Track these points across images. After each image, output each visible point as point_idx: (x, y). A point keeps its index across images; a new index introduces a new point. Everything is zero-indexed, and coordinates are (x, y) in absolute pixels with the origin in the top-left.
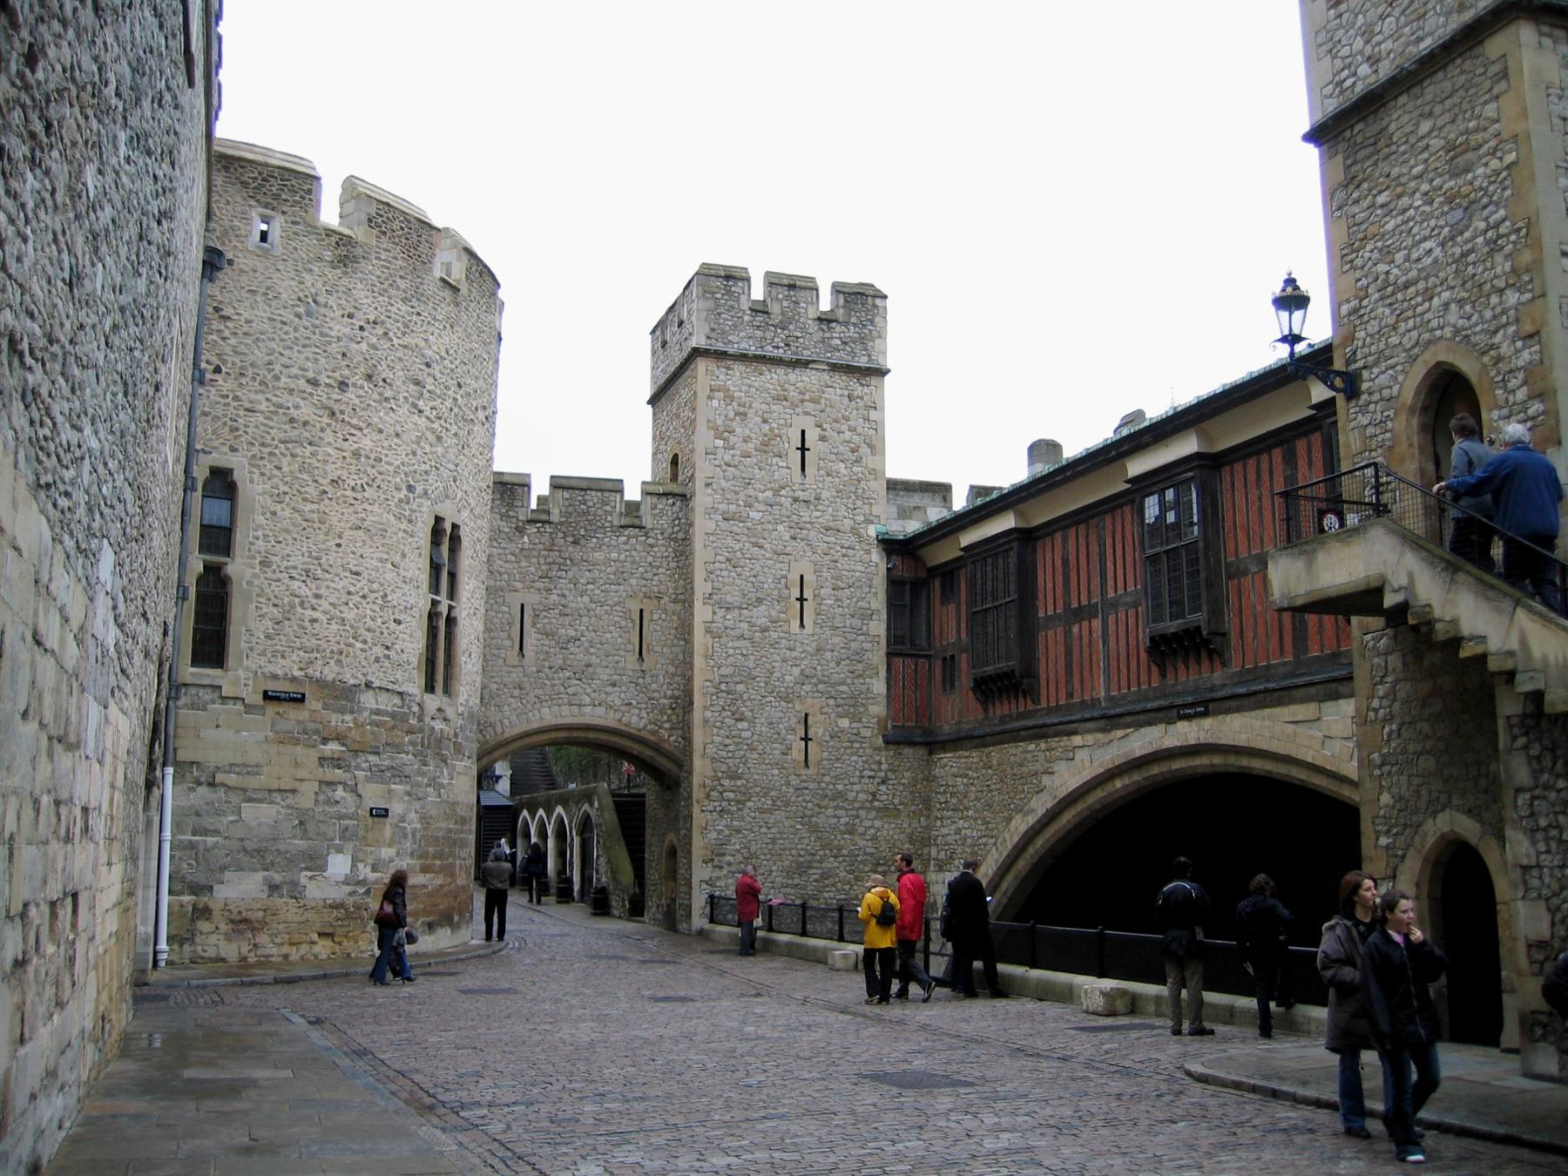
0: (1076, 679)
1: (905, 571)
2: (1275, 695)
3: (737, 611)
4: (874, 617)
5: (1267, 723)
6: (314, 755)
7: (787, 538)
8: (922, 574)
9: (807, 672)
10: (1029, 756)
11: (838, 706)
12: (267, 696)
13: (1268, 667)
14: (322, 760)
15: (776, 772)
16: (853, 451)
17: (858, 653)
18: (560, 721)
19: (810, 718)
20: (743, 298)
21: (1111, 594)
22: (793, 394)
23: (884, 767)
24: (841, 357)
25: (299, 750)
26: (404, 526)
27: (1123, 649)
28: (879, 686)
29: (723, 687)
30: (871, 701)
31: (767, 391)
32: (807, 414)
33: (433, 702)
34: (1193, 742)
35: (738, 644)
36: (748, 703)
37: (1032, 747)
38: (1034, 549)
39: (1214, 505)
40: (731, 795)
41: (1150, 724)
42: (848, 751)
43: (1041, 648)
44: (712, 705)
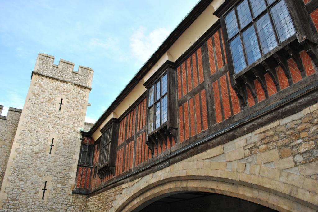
0: (126, 164)
1: (87, 142)
2: (199, 148)
3: (28, 146)
4: (75, 154)
5: (195, 162)
7: (51, 127)
8: (93, 143)
9: (49, 168)
10: (110, 194)
11: (58, 180)
13: (196, 137)
15: (31, 200)
16: (77, 107)
17: (68, 164)
19: (47, 183)
20: (51, 63)
21: (138, 130)
22: (61, 89)
23: (71, 201)
24: (76, 82)
27: (140, 149)
28: (74, 175)
29: (17, 169)
30: (70, 179)
31: (53, 87)
32: (64, 95)
34: (162, 178)
35: (26, 156)
36: (25, 176)
37: (111, 191)
38: (119, 126)
39: (174, 80)
40: (12, 207)
41: (147, 174)
42: (59, 195)
43: (117, 157)
44: (12, 175)
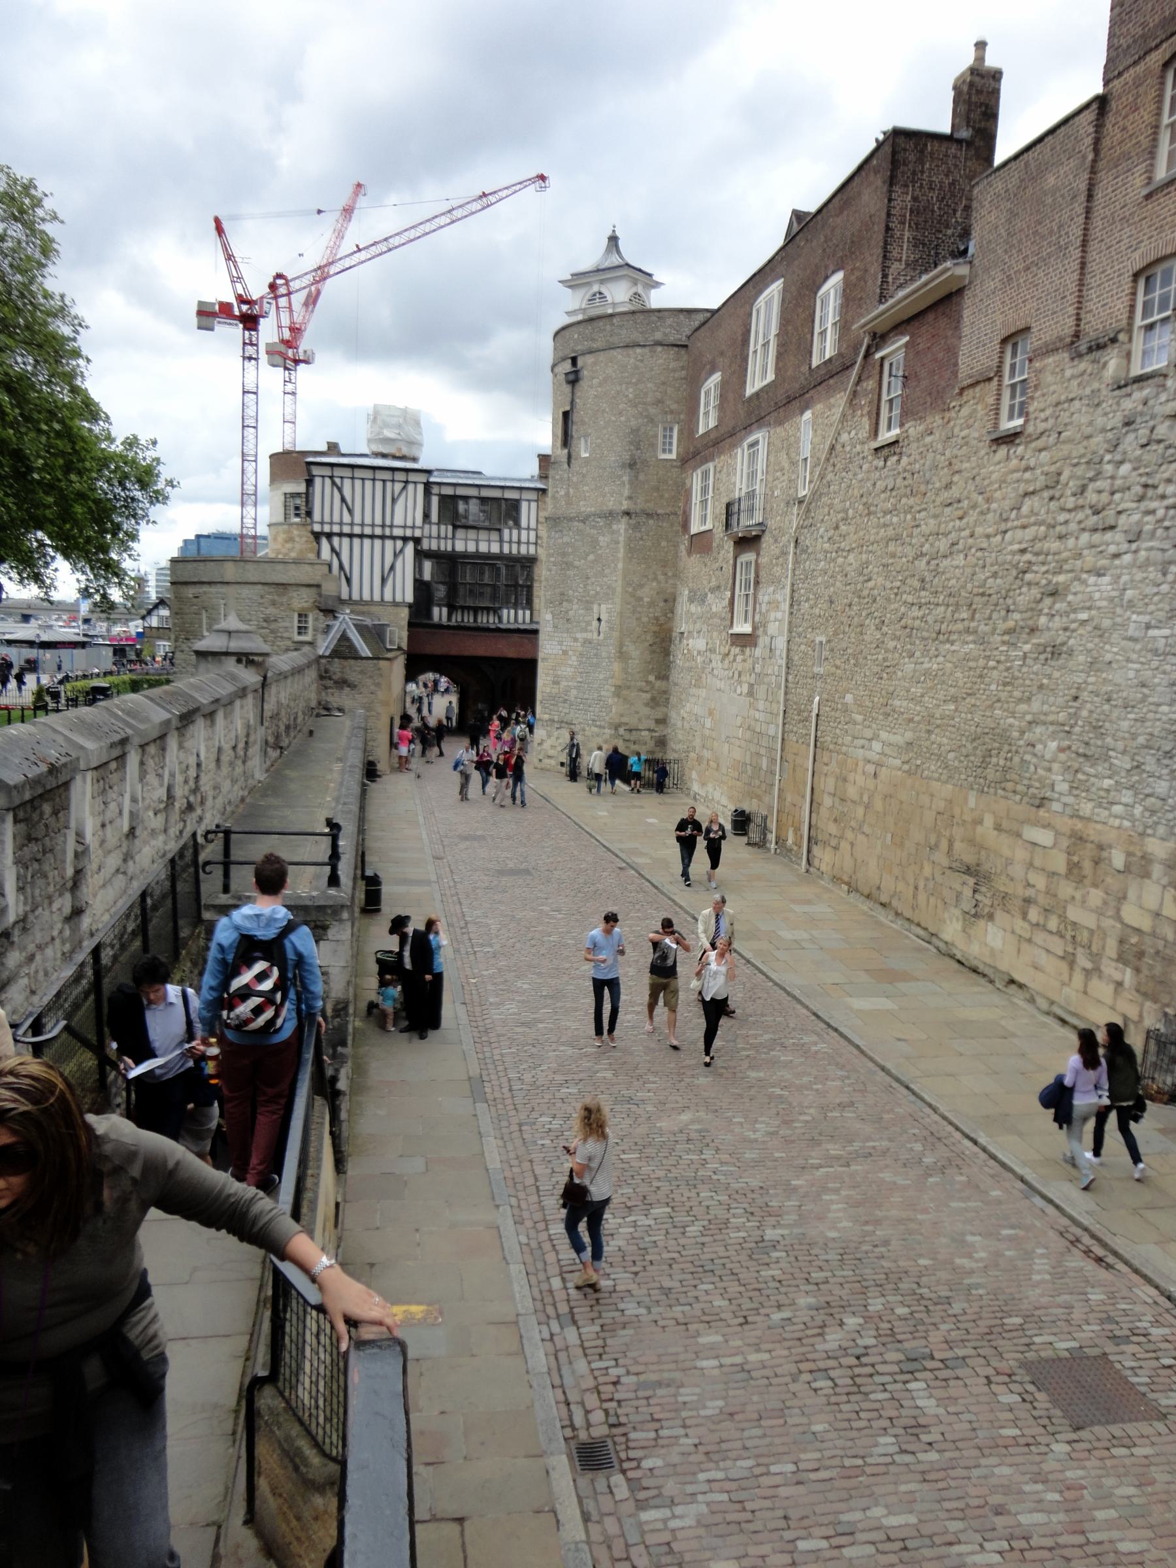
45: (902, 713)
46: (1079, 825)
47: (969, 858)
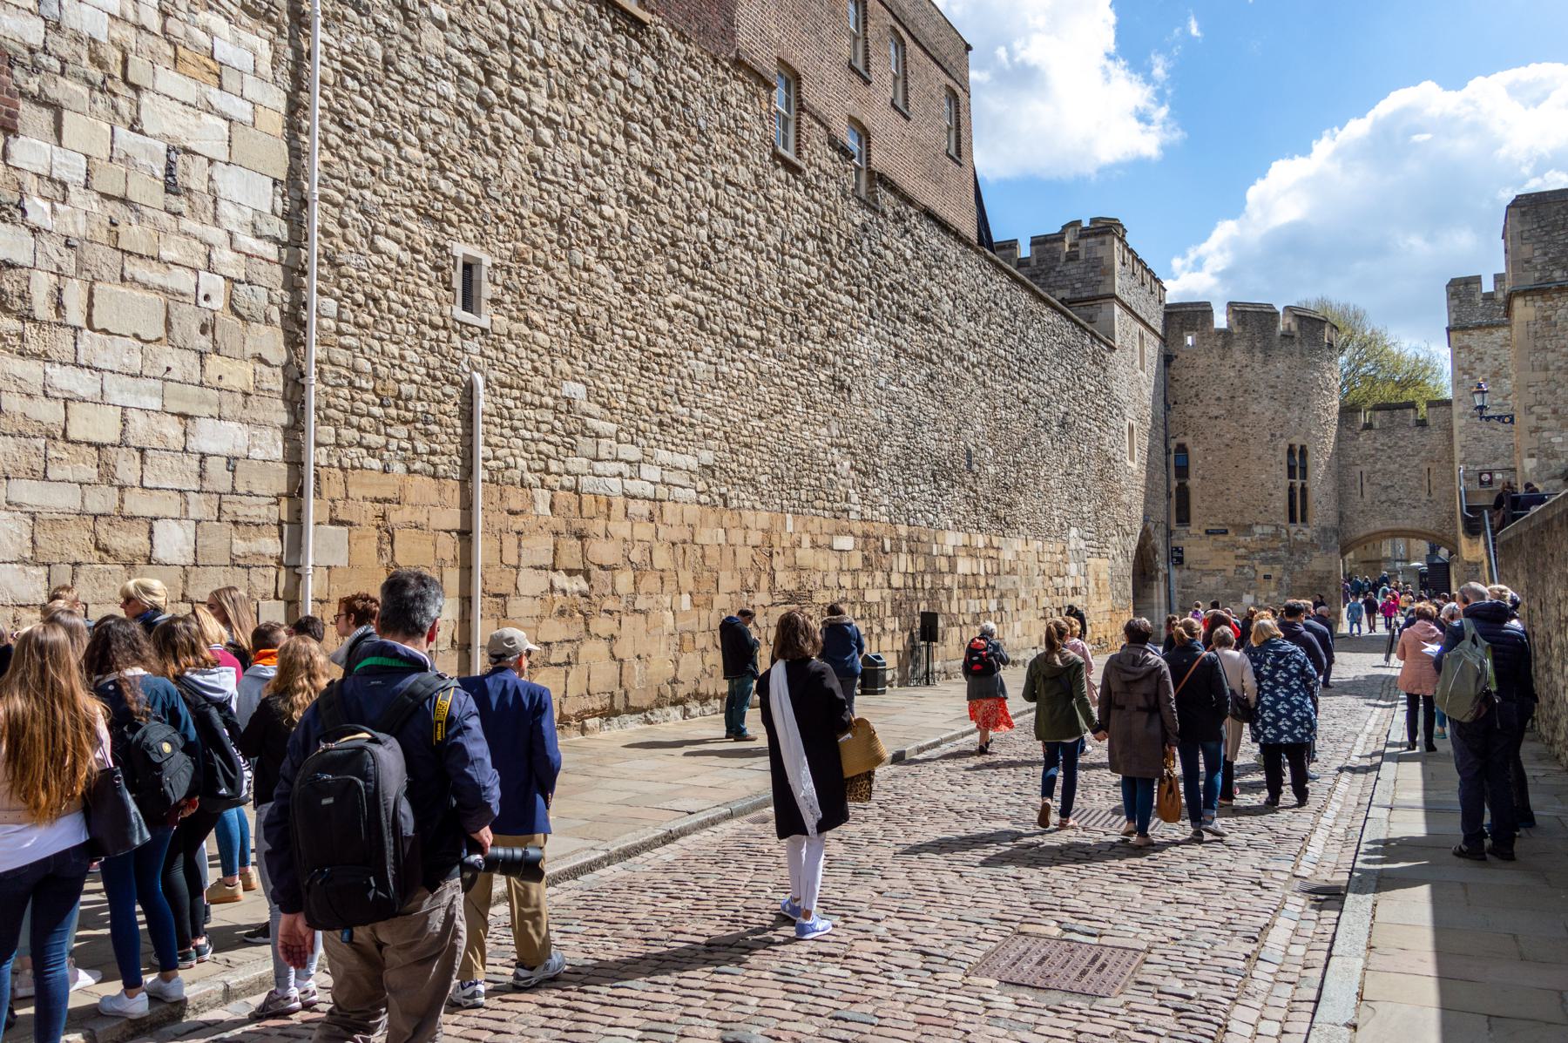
6: (1233, 555)
12: (1207, 532)
14: (1237, 557)
18: (1387, 528)
25: (1226, 553)
26: (1271, 452)
33: (1293, 529)
45: (692, 425)
46: (867, 526)
47: (792, 586)
